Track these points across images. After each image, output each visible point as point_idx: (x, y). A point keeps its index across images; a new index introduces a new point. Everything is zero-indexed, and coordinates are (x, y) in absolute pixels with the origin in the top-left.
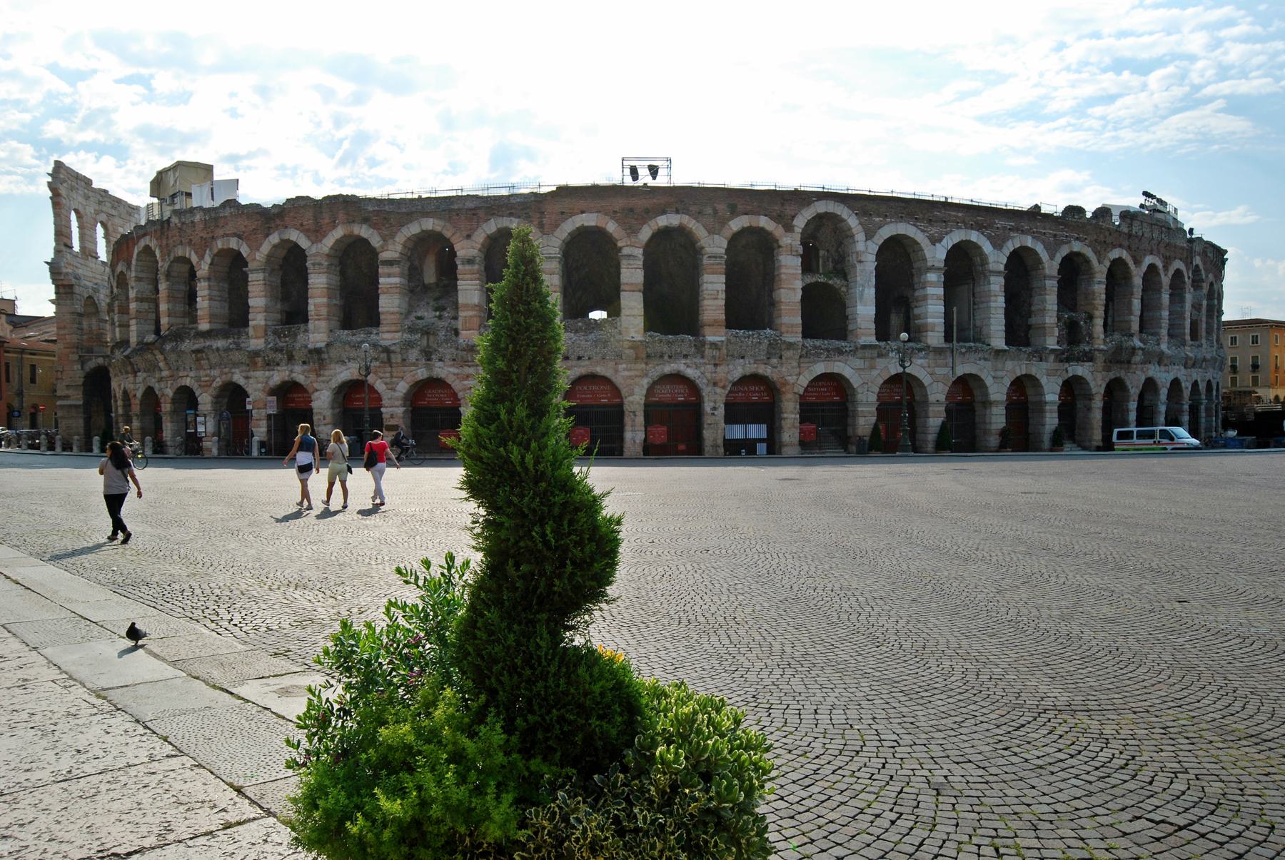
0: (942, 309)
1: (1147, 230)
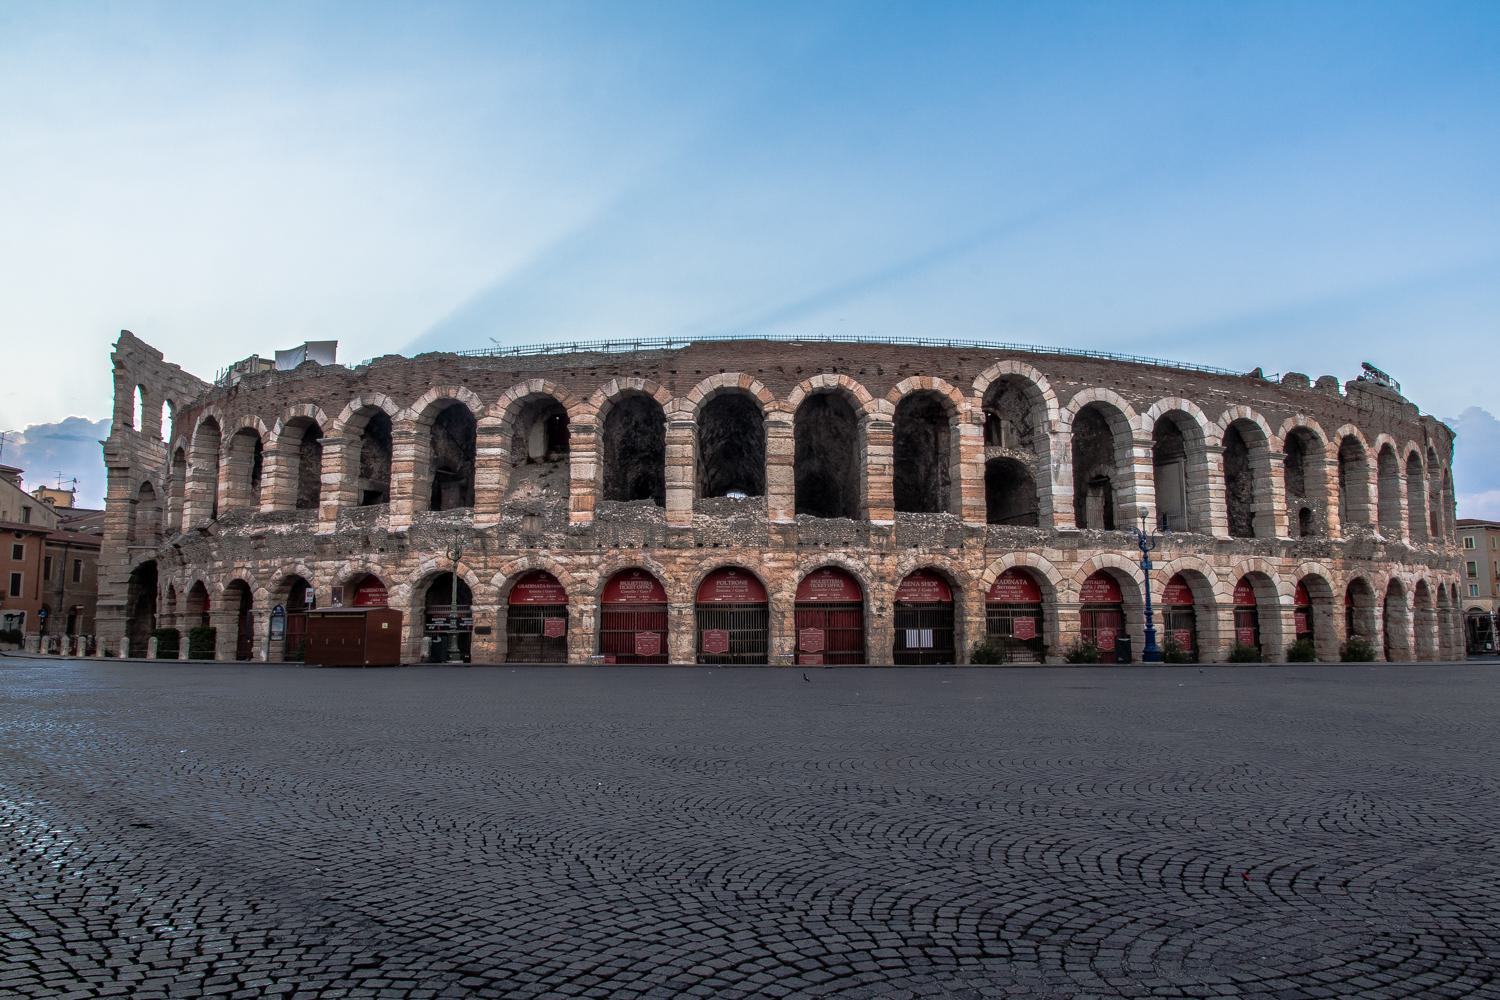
0: (1152, 490)
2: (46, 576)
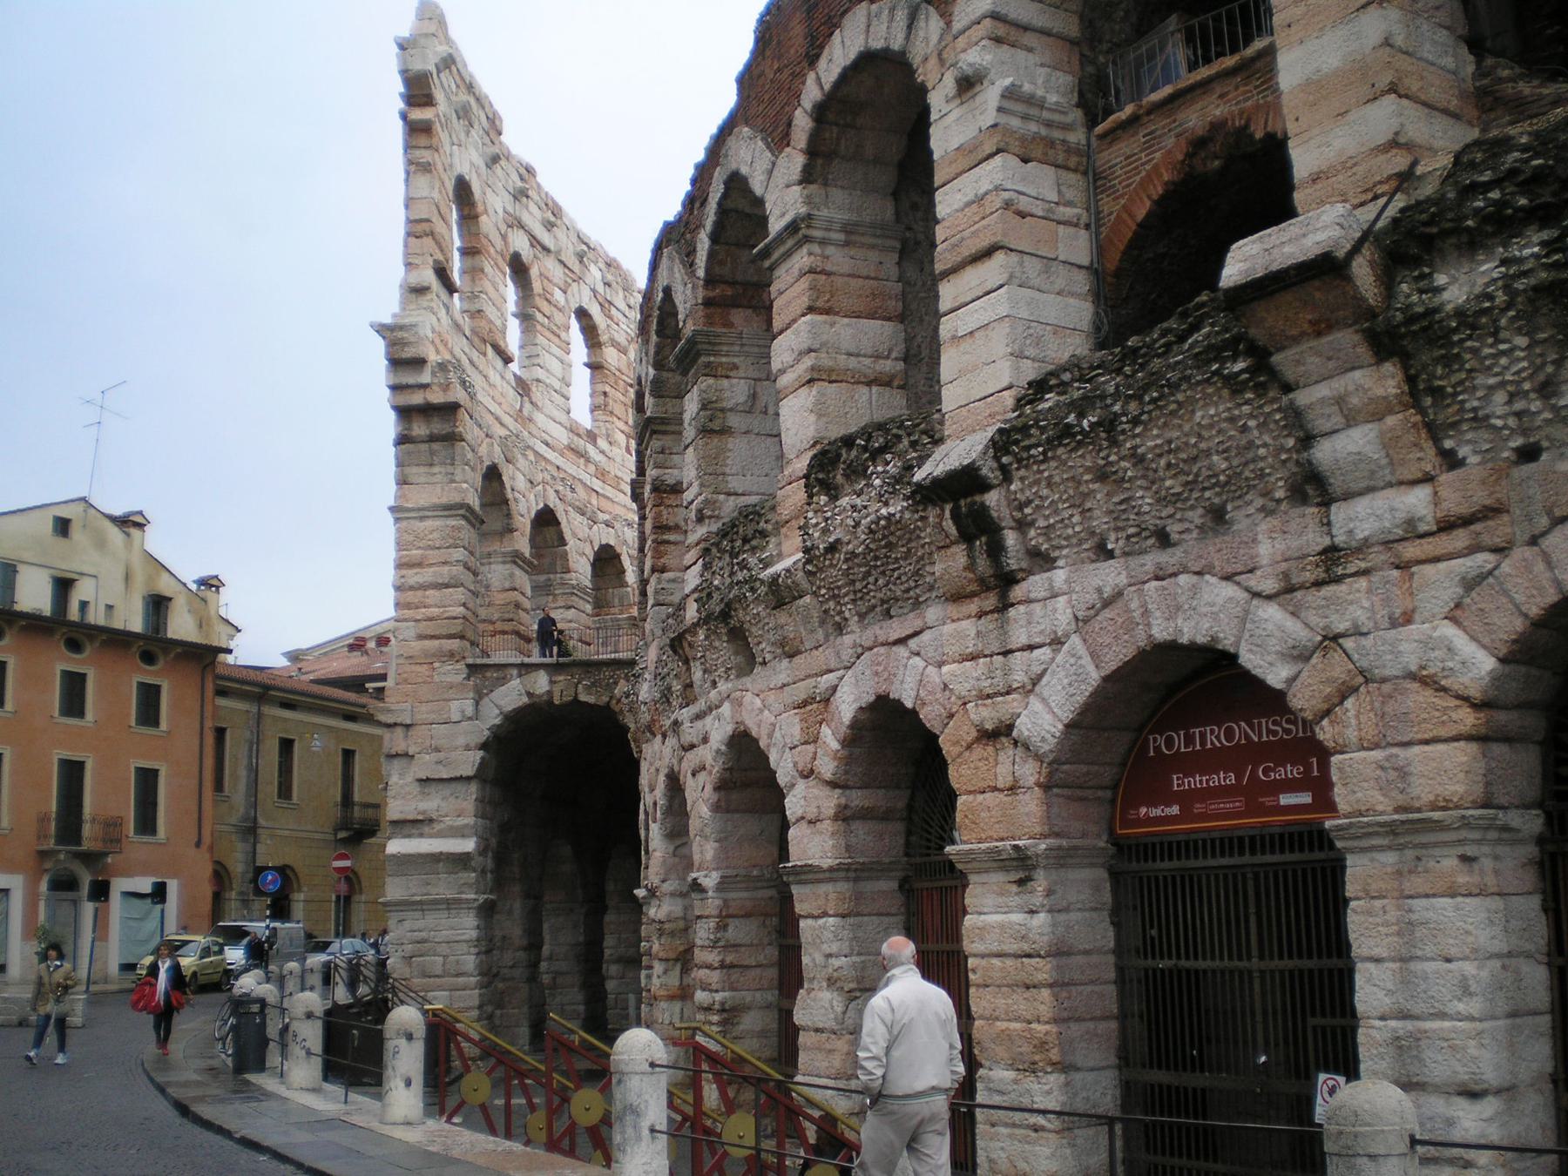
2: (219, 785)
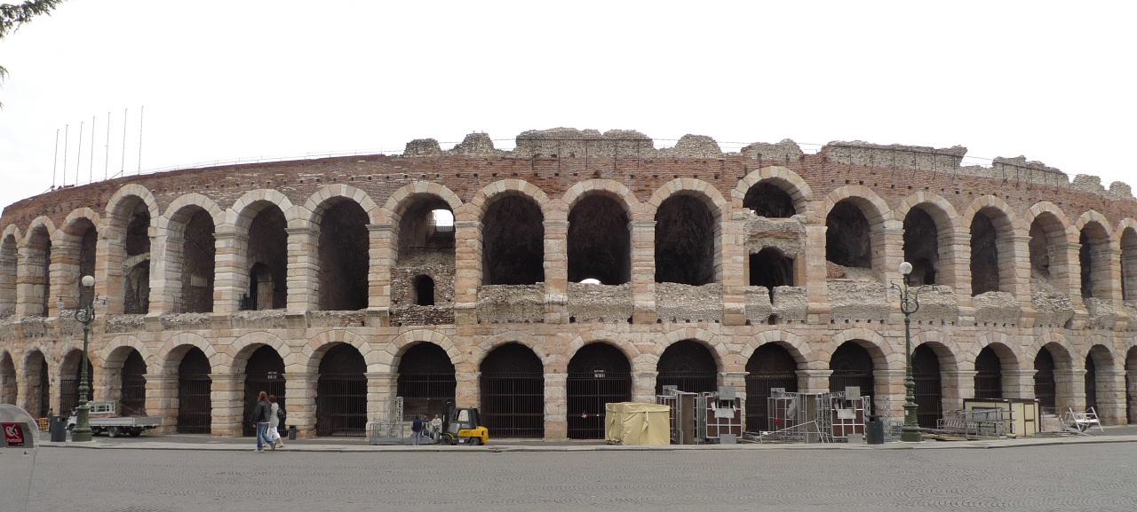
1: (580, 152)
